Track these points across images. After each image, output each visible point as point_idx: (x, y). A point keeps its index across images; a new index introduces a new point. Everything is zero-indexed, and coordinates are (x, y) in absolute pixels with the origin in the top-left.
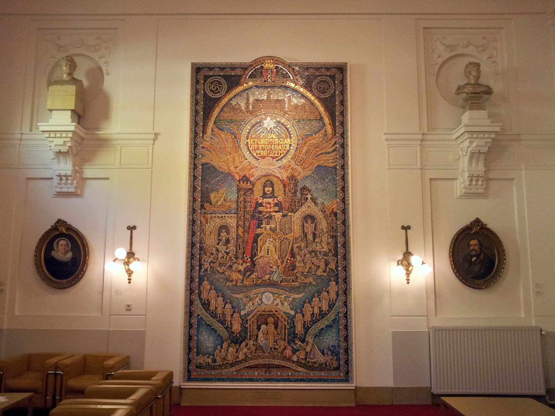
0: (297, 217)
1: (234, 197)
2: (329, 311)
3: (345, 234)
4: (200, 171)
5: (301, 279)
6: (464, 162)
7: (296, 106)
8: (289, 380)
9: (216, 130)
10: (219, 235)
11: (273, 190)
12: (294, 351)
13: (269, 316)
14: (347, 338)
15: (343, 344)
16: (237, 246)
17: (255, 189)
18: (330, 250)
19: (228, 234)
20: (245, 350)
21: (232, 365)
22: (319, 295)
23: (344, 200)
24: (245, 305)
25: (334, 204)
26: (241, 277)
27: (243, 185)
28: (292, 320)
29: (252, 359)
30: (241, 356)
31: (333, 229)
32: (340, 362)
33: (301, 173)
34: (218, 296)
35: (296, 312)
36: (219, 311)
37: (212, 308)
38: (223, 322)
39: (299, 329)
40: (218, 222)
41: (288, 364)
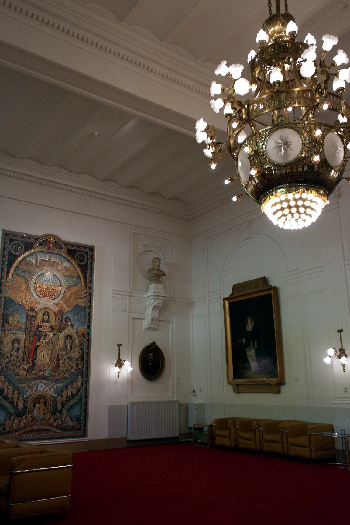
0: (62, 336)
1: (24, 321)
2: (77, 394)
4: (3, 302)
5: (62, 375)
6: (149, 311)
7: (65, 268)
8: (50, 438)
9: (15, 276)
10: (13, 345)
11: (49, 318)
12: (55, 420)
13: (41, 398)
14: (86, 411)
16: (24, 353)
17: (38, 316)
18: (79, 357)
19: (19, 344)
20: (25, 421)
21: (16, 431)
22: (72, 385)
23: (89, 327)
24: (27, 391)
25: (83, 329)
26: (25, 373)
27: (30, 313)
29: (29, 426)
30: (22, 425)
31: (82, 344)
32: (81, 424)
33: (66, 309)
34: (10, 386)
35: (58, 395)
36: (10, 395)
37: (5, 393)
38: (11, 403)
39: (59, 405)
40: (13, 336)
41: (51, 428)
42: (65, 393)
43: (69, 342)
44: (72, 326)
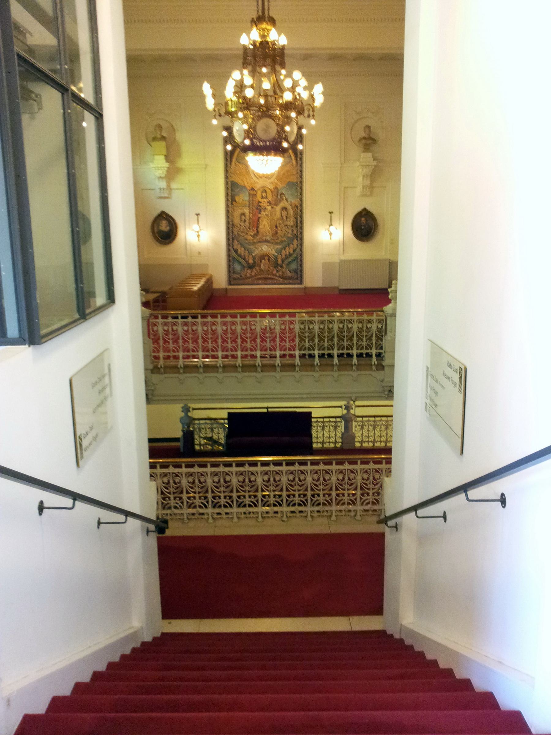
0: (278, 209)
1: (247, 198)
3: (301, 217)
5: (280, 238)
6: (361, 179)
8: (275, 284)
9: (237, 163)
10: (241, 218)
12: (277, 271)
13: (266, 256)
14: (301, 266)
15: (299, 268)
16: (250, 223)
20: (255, 271)
23: (301, 200)
25: (296, 201)
27: (251, 192)
28: (276, 258)
30: (253, 274)
33: (280, 186)
36: (243, 254)
37: (239, 253)
38: (244, 259)
39: (280, 261)
40: (240, 211)
42: (284, 253)
43: (284, 213)
44: (286, 200)
